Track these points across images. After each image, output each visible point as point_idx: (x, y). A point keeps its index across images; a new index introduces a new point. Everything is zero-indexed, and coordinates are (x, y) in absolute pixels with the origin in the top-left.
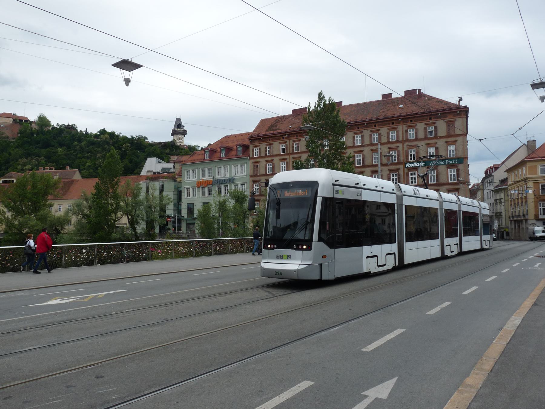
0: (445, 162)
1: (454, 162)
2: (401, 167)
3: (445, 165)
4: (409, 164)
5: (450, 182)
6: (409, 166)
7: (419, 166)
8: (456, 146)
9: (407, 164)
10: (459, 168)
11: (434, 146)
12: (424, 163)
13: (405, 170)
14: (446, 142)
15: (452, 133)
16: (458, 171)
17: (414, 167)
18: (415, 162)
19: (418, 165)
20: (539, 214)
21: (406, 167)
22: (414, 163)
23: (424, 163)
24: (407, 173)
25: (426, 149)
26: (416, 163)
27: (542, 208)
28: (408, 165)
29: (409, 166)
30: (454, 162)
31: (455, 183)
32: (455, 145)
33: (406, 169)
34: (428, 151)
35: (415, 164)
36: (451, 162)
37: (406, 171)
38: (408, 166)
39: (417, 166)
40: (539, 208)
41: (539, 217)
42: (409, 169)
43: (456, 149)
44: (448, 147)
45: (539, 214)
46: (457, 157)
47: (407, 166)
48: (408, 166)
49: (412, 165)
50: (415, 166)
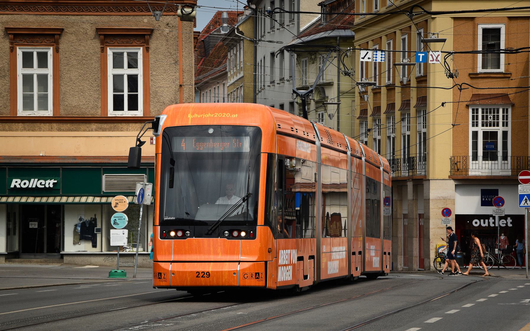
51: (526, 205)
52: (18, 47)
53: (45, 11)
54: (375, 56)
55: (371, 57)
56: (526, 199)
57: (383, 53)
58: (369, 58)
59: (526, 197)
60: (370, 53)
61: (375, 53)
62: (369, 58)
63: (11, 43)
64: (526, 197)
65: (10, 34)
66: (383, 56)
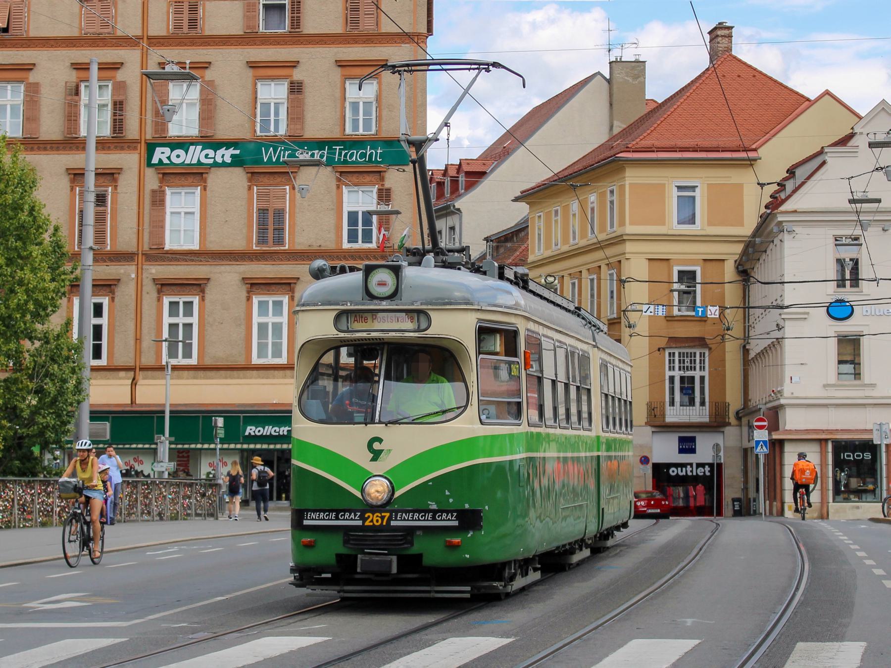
0: (332, 152)
1: (371, 154)
2: (129, 161)
3: (329, 169)
4: (167, 150)
5: (346, 245)
6: (169, 158)
7: (211, 161)
8: (380, 84)
9: (159, 150)
10: (387, 185)
11: (285, 77)
12: (238, 152)
13: (147, 179)
14: (341, 64)
15: (367, 25)
16: (385, 195)
17: (190, 164)
18: (192, 144)
19: (207, 156)
20: (667, 403)
21: (149, 164)
22: (192, 148)
23: (238, 152)
24: (153, 191)
25: (250, 86)
26: (199, 148)
27: (677, 374)
28: (161, 154)
29: (169, 158)
30: (371, 154)
31: (370, 251)
32: (375, 82)
33: (150, 173)
34: (259, 97)
35: (196, 155)
36: (355, 155)
37: (152, 180)
38: (160, 160)
39: (204, 160)
40: (668, 373)
41: (663, 416)
42: (164, 174)
43: (378, 99)
44: (347, 83)
45: (667, 403)
46: (383, 135)
47: (155, 160)
48: (160, 160)
49: (179, 157)
50: (195, 161)
51: (762, 450)
52: (254, 296)
53: (282, 260)
54: (656, 310)
55: (653, 311)
56: (762, 445)
57: (664, 308)
58: (651, 312)
59: (761, 442)
60: (652, 307)
61: (657, 308)
62: (651, 312)
63: (248, 292)
64: (761, 442)
65: (247, 283)
66: (664, 310)
